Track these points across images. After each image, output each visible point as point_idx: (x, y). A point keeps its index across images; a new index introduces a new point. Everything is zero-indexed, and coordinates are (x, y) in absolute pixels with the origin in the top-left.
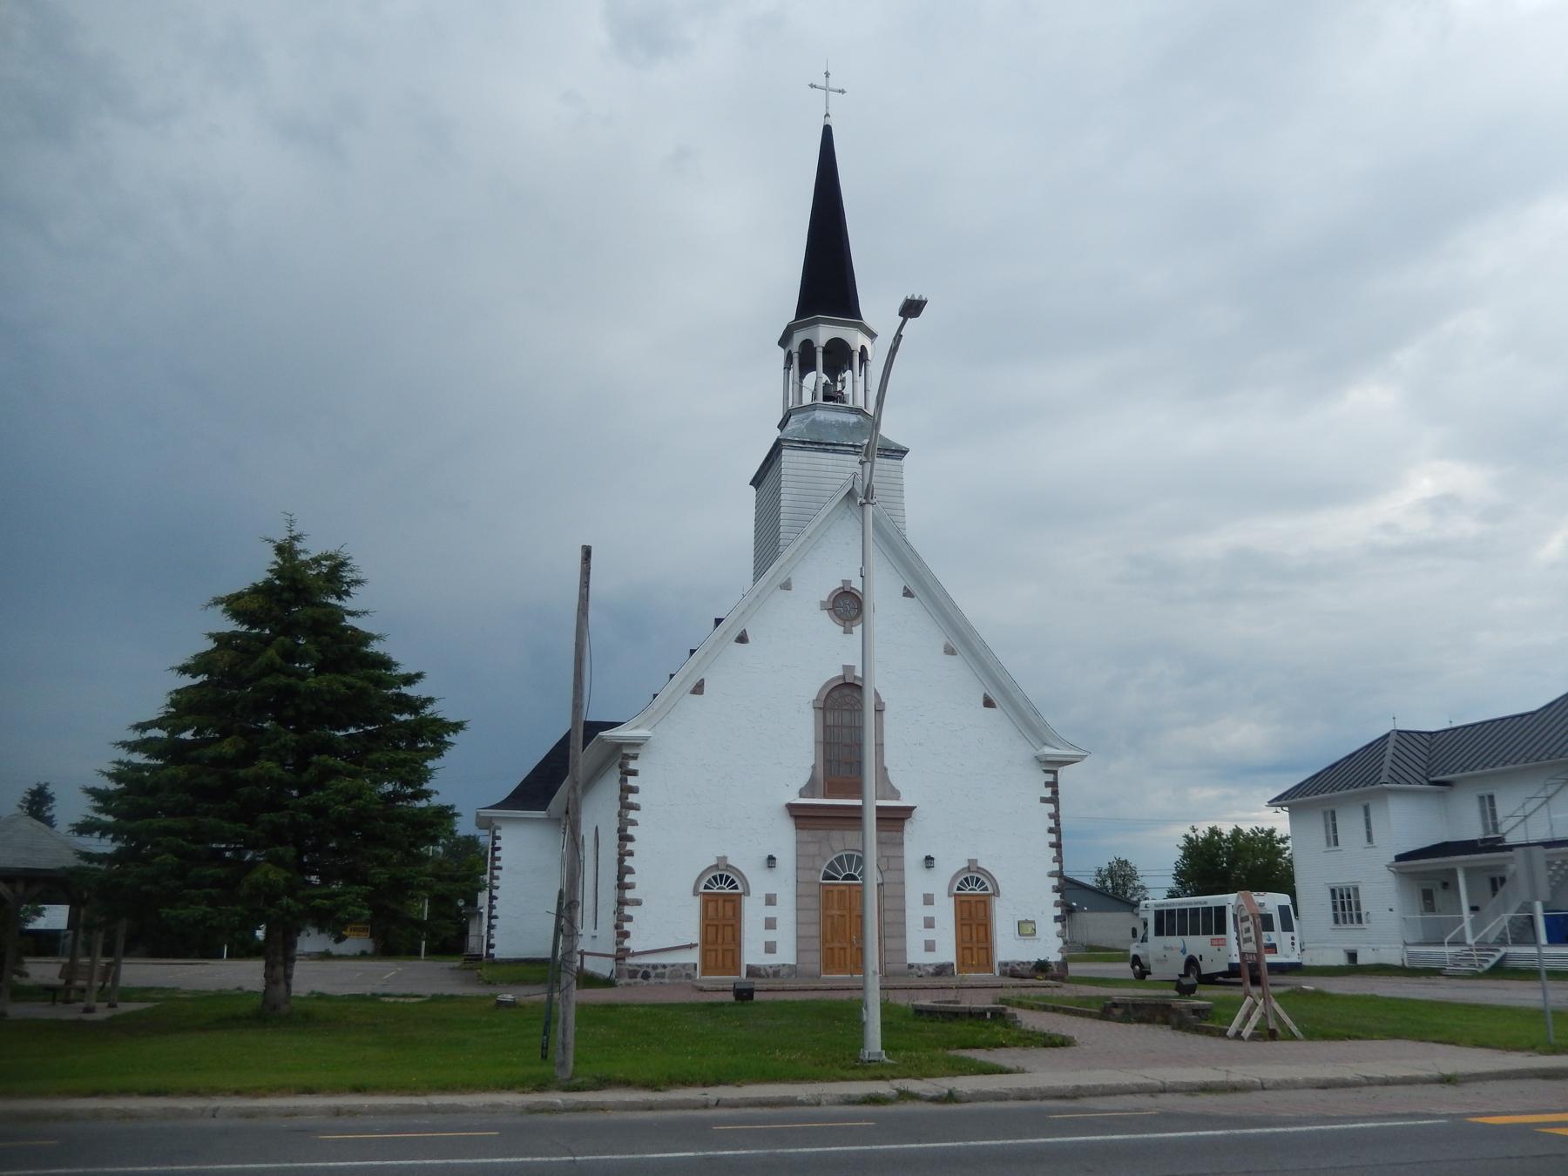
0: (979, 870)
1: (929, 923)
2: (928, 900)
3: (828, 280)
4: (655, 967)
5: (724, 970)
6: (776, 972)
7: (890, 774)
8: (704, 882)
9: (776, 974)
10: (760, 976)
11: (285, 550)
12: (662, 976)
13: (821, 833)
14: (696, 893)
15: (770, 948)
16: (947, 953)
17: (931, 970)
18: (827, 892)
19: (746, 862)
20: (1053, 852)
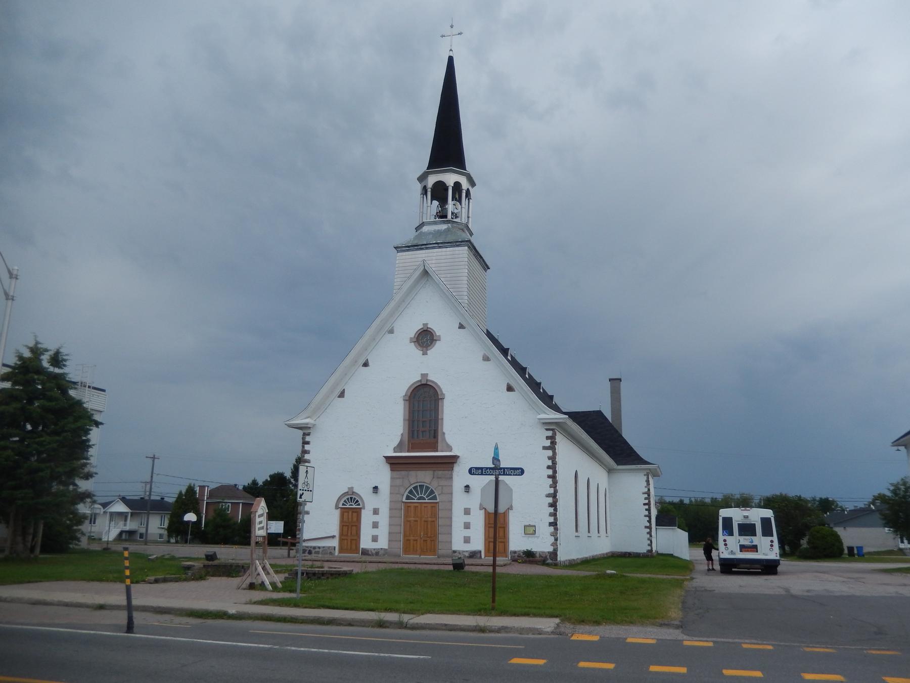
0: (353, 493)
1: (467, 526)
2: (467, 512)
3: (447, 147)
4: (314, 548)
5: (351, 551)
6: (377, 553)
7: (446, 436)
8: (342, 502)
9: (377, 554)
10: (368, 555)
11: (37, 343)
12: (318, 553)
13: (403, 473)
14: (337, 507)
15: (375, 539)
16: (478, 543)
17: (467, 554)
18: (407, 506)
19: (364, 492)
20: (550, 481)
